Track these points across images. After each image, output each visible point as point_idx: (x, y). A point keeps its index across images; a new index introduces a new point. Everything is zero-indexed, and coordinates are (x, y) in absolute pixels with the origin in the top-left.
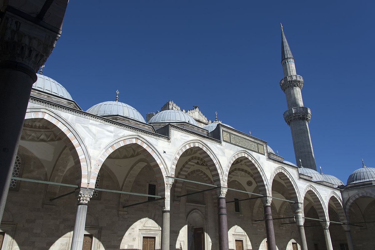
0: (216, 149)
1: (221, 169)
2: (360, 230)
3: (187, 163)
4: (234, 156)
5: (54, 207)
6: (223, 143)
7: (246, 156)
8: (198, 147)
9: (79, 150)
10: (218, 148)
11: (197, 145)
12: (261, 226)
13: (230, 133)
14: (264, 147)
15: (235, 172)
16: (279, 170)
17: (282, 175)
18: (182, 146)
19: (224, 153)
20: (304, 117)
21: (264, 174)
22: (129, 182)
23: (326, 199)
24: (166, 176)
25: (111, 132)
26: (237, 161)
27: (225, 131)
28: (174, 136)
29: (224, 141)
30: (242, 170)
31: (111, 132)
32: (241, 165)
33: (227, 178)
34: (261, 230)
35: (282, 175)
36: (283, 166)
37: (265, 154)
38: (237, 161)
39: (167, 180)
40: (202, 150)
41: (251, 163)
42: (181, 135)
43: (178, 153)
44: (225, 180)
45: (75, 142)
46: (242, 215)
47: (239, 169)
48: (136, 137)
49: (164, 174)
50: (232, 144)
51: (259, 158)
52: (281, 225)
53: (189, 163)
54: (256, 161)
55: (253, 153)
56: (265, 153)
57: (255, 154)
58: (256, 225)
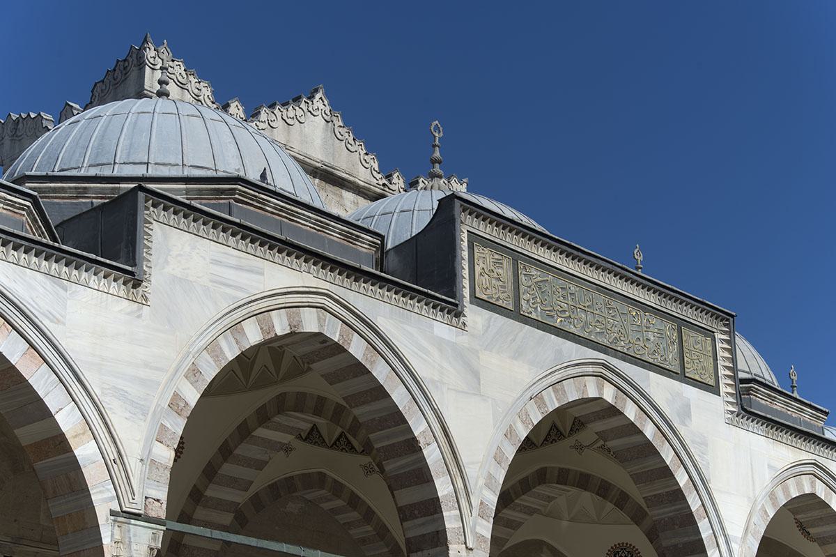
0: (425, 344)
1: (454, 470)
3: (244, 432)
4: (537, 398)
6: (475, 316)
7: (609, 394)
8: (320, 334)
10: (440, 343)
11: (310, 322)
13: (516, 256)
14: (719, 345)
15: (541, 490)
16: (799, 485)
17: (817, 514)
18: (214, 331)
19: (476, 375)
24: (113, 513)
26: (554, 426)
28: (167, 262)
29: (476, 300)
30: (584, 481)
32: (580, 448)
33: (485, 529)
35: (817, 514)
36: (821, 460)
37: (723, 389)
38: (554, 426)
39: (117, 537)
40: (340, 356)
41: (635, 439)
42: (216, 262)
43: (194, 372)
44: (480, 538)
47: (563, 477)
49: (103, 500)
50: (526, 320)
51: (686, 412)
53: (261, 432)
56: (722, 381)
57: (659, 387)
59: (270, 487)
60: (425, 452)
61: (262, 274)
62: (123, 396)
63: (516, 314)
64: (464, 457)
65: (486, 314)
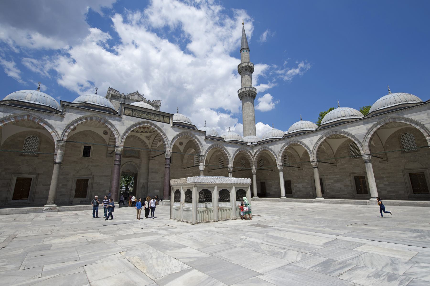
1: (118, 134)
2: (271, 173)
12: (191, 171)
20: (250, 95)
21: (166, 137)
23: (232, 153)
24: (57, 140)
27: (127, 108)
34: (189, 174)
37: (171, 123)
46: (173, 165)
52: (209, 170)
55: (156, 122)
56: (171, 122)
57: (158, 124)
58: (185, 171)
60: (113, 132)
61: (85, 113)
62: (59, 128)
64: (120, 132)
65: (126, 116)
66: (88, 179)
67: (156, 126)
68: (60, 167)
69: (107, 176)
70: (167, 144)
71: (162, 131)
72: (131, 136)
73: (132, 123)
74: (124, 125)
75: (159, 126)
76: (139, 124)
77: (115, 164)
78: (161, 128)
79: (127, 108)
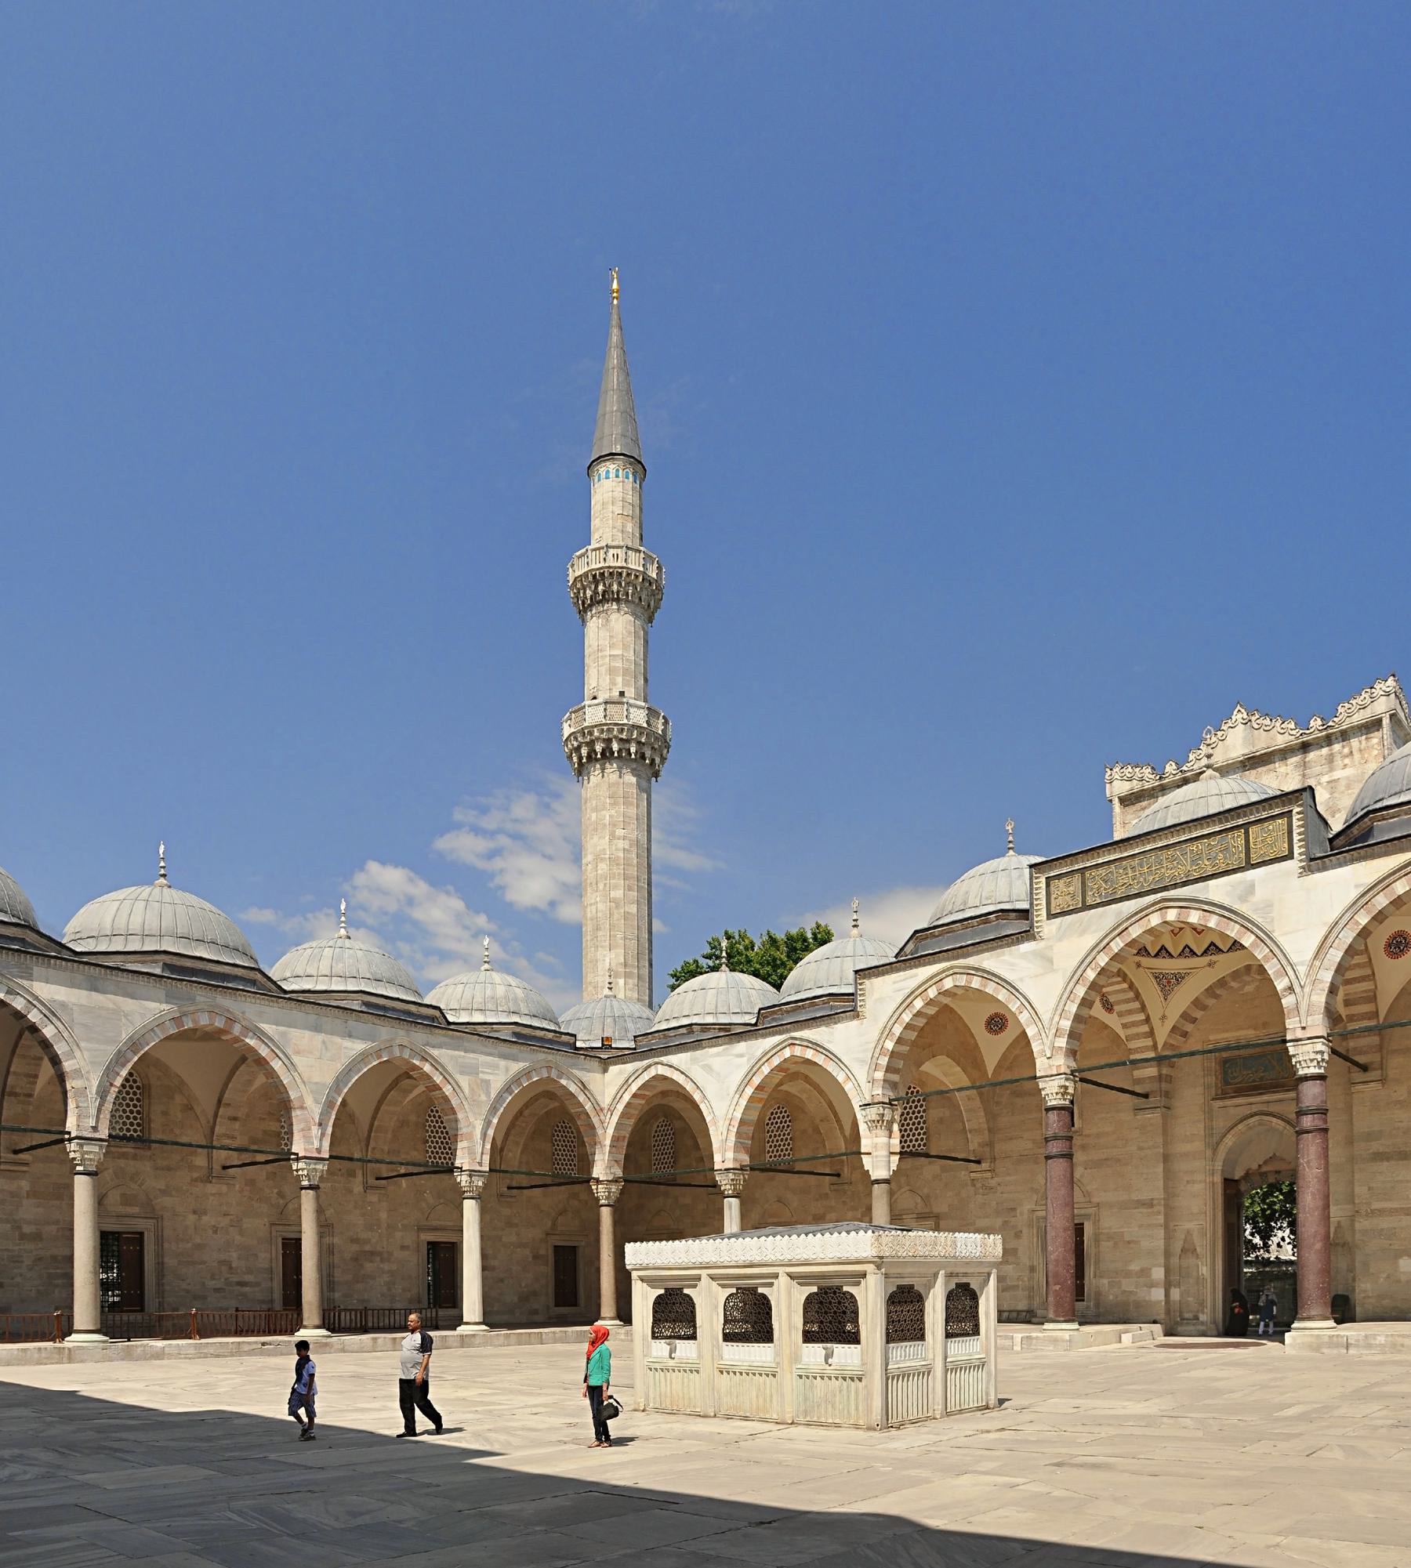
5: (846, 1187)
7: (1172, 915)
9: (702, 1107)
21: (1277, 950)
22: (969, 1099)
25: (742, 1056)
29: (1051, 916)
31: (742, 1056)
45: (697, 1097)
48: (790, 1041)
54: (1226, 914)
59: (1207, 990)
63: (1086, 907)
66: (1083, 1224)
67: (1209, 906)
68: (891, 1193)
69: (1150, 1204)
70: (1285, 990)
71: (1247, 924)
72: (1236, 975)
73: (1090, 940)
74: (1055, 967)
75: (1226, 901)
76: (1120, 929)
77: (1048, 1158)
78: (1236, 906)
79: (1059, 877)
